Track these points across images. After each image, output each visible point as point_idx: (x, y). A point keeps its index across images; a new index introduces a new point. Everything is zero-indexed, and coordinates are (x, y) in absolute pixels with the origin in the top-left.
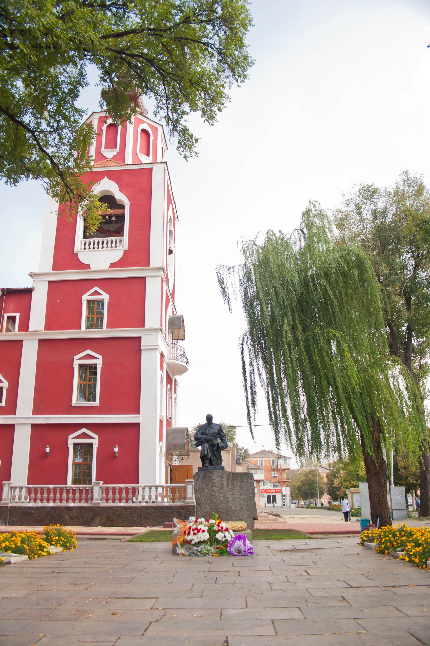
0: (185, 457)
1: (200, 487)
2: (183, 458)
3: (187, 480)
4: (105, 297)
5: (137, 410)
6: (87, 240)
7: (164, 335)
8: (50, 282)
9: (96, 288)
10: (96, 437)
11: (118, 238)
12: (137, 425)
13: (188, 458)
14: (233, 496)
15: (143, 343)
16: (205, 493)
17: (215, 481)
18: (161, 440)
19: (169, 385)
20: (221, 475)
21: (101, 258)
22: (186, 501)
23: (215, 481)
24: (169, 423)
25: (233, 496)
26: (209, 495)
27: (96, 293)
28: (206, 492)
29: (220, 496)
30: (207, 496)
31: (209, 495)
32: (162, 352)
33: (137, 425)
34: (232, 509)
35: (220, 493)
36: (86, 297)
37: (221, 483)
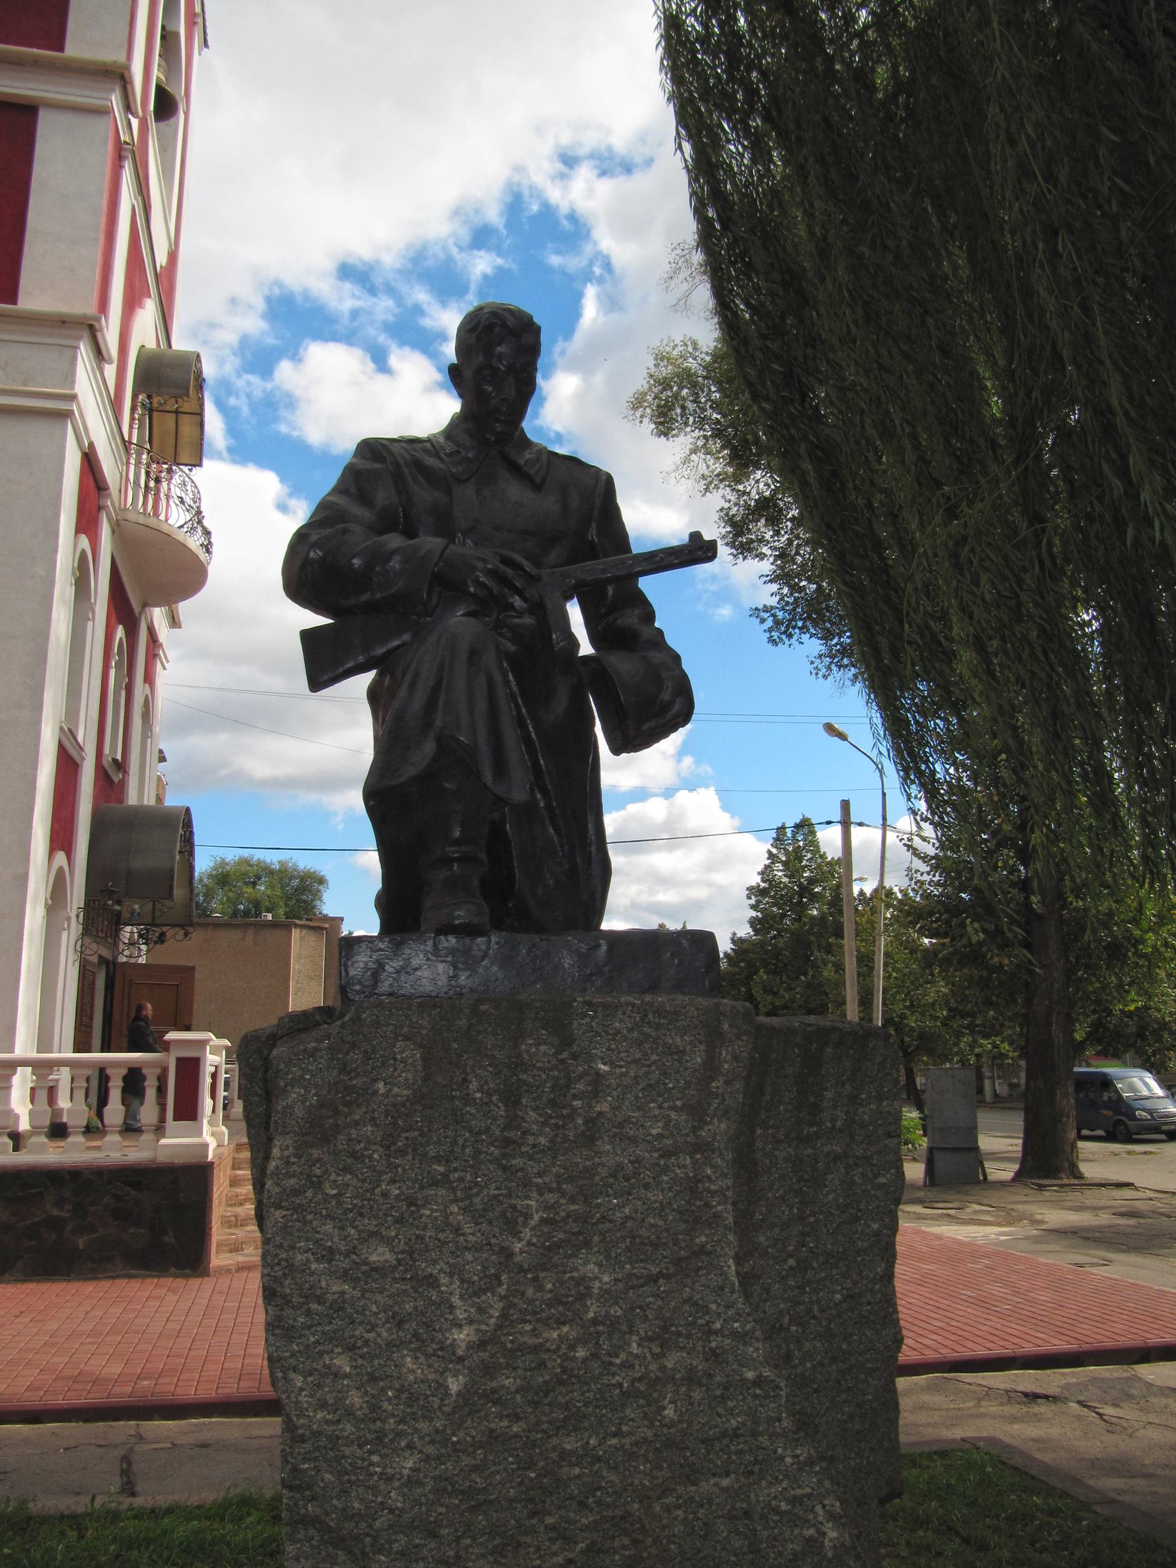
0: (170, 932)
1: (380, 1255)
2: (163, 934)
3: (172, 1036)
7: (110, 371)
13: (186, 934)
16: (449, 1356)
17: (609, 1154)
18: (61, 838)
19: (120, 632)
22: (163, 1141)
24: (111, 780)
28: (462, 1336)
30: (469, 1403)
32: (91, 445)
34: (813, 1545)
35: (663, 1339)
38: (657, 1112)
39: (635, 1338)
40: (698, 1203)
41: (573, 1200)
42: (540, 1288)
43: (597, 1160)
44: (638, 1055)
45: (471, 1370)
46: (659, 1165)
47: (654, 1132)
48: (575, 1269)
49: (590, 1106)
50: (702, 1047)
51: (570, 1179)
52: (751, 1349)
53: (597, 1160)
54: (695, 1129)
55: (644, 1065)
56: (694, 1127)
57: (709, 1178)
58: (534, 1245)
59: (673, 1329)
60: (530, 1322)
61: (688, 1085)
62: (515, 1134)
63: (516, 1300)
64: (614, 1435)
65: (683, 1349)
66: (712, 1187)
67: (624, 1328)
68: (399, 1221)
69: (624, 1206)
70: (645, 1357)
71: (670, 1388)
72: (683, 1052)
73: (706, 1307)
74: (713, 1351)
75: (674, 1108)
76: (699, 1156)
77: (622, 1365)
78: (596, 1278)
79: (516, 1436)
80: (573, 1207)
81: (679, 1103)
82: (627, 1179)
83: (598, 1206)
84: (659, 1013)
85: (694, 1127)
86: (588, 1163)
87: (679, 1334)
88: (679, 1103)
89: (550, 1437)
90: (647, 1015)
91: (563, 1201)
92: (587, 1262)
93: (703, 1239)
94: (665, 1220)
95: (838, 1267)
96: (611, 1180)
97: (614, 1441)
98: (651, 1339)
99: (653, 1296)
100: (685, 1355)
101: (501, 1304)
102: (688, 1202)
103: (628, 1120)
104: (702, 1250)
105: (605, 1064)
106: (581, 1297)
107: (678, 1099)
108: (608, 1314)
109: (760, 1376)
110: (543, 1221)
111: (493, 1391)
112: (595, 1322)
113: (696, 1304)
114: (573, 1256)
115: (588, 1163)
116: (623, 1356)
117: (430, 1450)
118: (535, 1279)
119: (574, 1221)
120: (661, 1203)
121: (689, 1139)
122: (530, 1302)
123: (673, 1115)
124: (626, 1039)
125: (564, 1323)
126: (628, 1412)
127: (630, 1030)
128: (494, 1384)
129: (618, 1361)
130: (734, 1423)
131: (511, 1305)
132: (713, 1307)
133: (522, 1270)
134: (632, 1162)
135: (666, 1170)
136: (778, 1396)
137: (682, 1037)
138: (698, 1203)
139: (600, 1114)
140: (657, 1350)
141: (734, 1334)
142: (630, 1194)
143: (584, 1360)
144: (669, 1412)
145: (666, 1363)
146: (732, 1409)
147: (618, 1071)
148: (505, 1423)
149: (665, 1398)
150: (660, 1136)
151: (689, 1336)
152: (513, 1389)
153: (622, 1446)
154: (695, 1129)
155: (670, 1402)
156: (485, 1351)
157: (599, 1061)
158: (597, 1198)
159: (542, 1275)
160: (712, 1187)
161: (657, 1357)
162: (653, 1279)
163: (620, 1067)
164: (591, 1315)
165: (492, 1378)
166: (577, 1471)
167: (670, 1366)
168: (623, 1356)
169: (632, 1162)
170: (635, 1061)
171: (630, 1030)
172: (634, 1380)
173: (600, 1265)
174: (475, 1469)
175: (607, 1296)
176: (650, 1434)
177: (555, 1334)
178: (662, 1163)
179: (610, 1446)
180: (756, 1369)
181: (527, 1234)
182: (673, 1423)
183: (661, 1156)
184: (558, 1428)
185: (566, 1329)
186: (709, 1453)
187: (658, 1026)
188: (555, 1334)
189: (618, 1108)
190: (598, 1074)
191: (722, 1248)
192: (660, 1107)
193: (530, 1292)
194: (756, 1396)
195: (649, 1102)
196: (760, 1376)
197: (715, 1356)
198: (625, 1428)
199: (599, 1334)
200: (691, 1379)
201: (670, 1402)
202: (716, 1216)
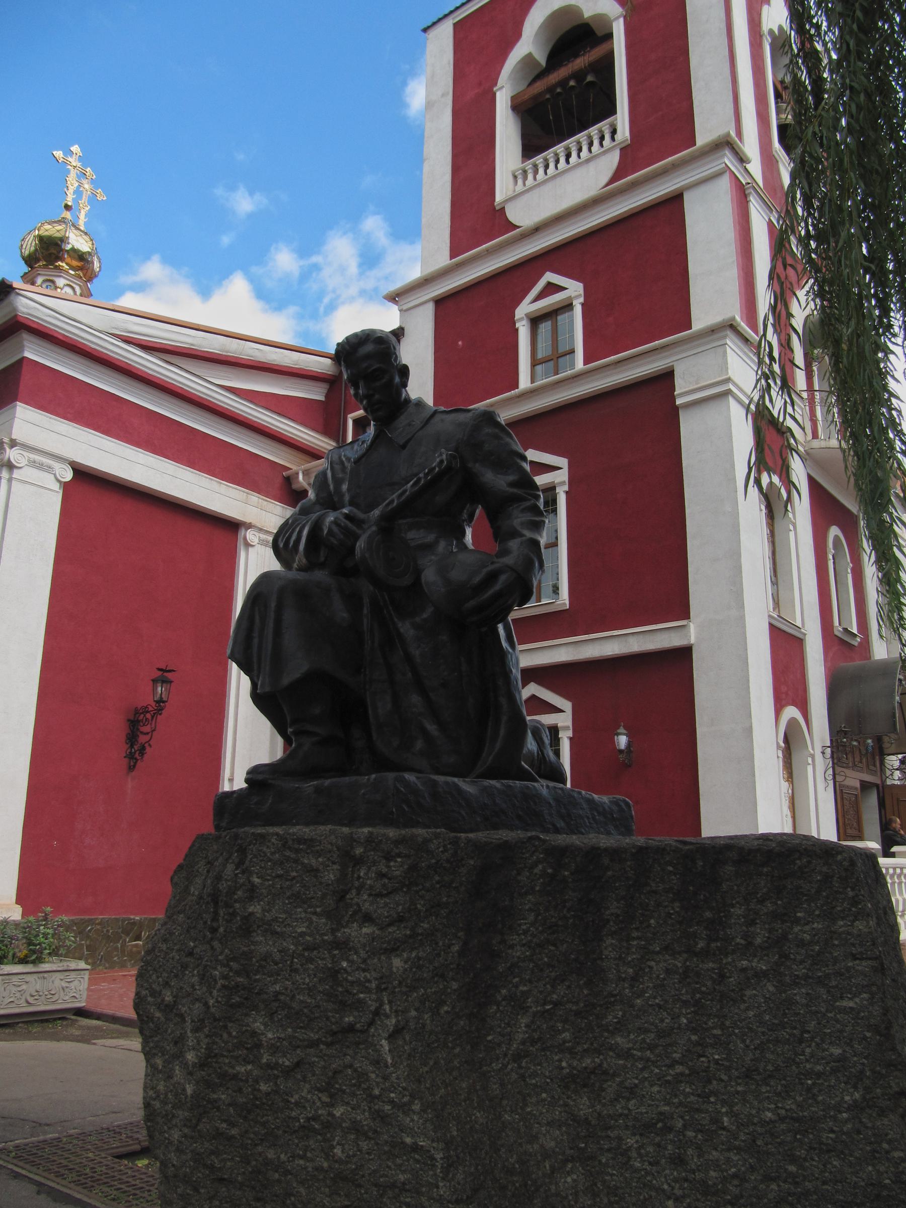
4: (574, 289)
5: (679, 607)
6: (529, 164)
8: (439, 302)
9: (550, 277)
10: (566, 705)
11: (604, 125)
12: (684, 654)
14: (583, 1105)
15: (681, 385)
20: (330, 876)
21: (559, 189)
23: (263, 945)
25: (583, 1105)
26: (223, 1096)
27: (552, 288)
29: (329, 1125)
31: (223, 1096)
33: (684, 654)
36: (525, 308)
37: (334, 974)
38: (303, 915)
39: (307, 1086)
40: (340, 989)
41: (238, 973)
42: (230, 1034)
43: (252, 947)
44: (280, 872)
45: (197, 1082)
46: (303, 955)
47: (299, 930)
48: (248, 1025)
49: (245, 909)
50: (335, 867)
51: (234, 959)
52: (408, 1119)
53: (252, 947)
54: (333, 931)
55: (287, 880)
56: (332, 929)
57: (345, 970)
58: (220, 1002)
59: (337, 1086)
60: (227, 1057)
61: (324, 896)
62: (215, 924)
63: (217, 1040)
64: (301, 1157)
65: (348, 1104)
66: (349, 978)
67: (299, 1077)
68: (176, 976)
69: (275, 983)
70: (314, 1103)
71: (339, 1132)
72: (317, 870)
73: (367, 1074)
74: (378, 1111)
75: (315, 913)
76: (336, 952)
77: (297, 1104)
78: (263, 1034)
79: (233, 1137)
80: (239, 979)
81: (318, 910)
82: (276, 964)
83: (256, 981)
84: (301, 841)
85: (332, 929)
86: (245, 949)
87: (344, 1092)
88: (318, 910)
89: (256, 1145)
90: (286, 842)
91: (231, 974)
92: (255, 1021)
93: (351, 1019)
94: (315, 999)
95: (767, 1085)
96: (264, 963)
97: (301, 1162)
98: (319, 1090)
99: (317, 1057)
100: (349, 1109)
101: (207, 1040)
102: (331, 987)
103: (275, 919)
104: (351, 1028)
105: (258, 878)
106: (258, 1046)
107: (317, 907)
108: (277, 1063)
109: (415, 1144)
110: (224, 987)
111: (216, 1101)
112: (269, 1066)
113: (355, 1070)
114: (246, 1015)
115: (245, 949)
116: (296, 1097)
117: (186, 1130)
118: (225, 1027)
119: (243, 989)
120: (308, 984)
121: (326, 938)
122: (226, 1043)
123: (314, 918)
124: (270, 860)
125: (249, 1063)
126: (311, 1142)
127: (273, 853)
128: (215, 1096)
129: (293, 1101)
130: (402, 1177)
131: (214, 1043)
132: (373, 1076)
133: (215, 1020)
134: (280, 951)
135: (310, 960)
136: (434, 1165)
137: (317, 859)
138: (340, 989)
139: (251, 914)
140: (325, 1099)
141: (391, 1102)
142: (278, 975)
143: (268, 1094)
144: (338, 1151)
145: (335, 1112)
146: (401, 1165)
147: (267, 883)
148: (224, 1125)
149: (334, 1140)
150: (302, 934)
151: (354, 1095)
152: (226, 1103)
153: (306, 1168)
154: (333, 931)
155: (338, 1144)
156: (203, 1070)
157: (255, 876)
158: (256, 975)
159: (230, 1025)
160: (349, 978)
161: (326, 1105)
162: (314, 1044)
163: (268, 880)
164: (264, 1061)
165: (214, 1092)
166: (277, 1176)
167: (338, 1115)
168: (296, 1097)
169: (280, 951)
170: (278, 876)
171: (273, 853)
172: (308, 1119)
173: (266, 1025)
174: (212, 1153)
175: (274, 1049)
176: (325, 1165)
177: (243, 1069)
178: (306, 954)
179: (298, 1165)
180: (413, 1137)
181: (215, 993)
182: (339, 1161)
183: (304, 949)
184: (262, 1140)
185: (249, 1067)
186: (382, 1196)
187: (297, 851)
188: (243, 1069)
189: (269, 911)
190: (253, 885)
191: (376, 1029)
192: (306, 912)
193: (225, 1036)
194: (418, 1161)
195: (295, 907)
196: (415, 1144)
197: (380, 1116)
198: (309, 1155)
199: (277, 1077)
200: (356, 1128)
201: (338, 1144)
202: (360, 1001)
